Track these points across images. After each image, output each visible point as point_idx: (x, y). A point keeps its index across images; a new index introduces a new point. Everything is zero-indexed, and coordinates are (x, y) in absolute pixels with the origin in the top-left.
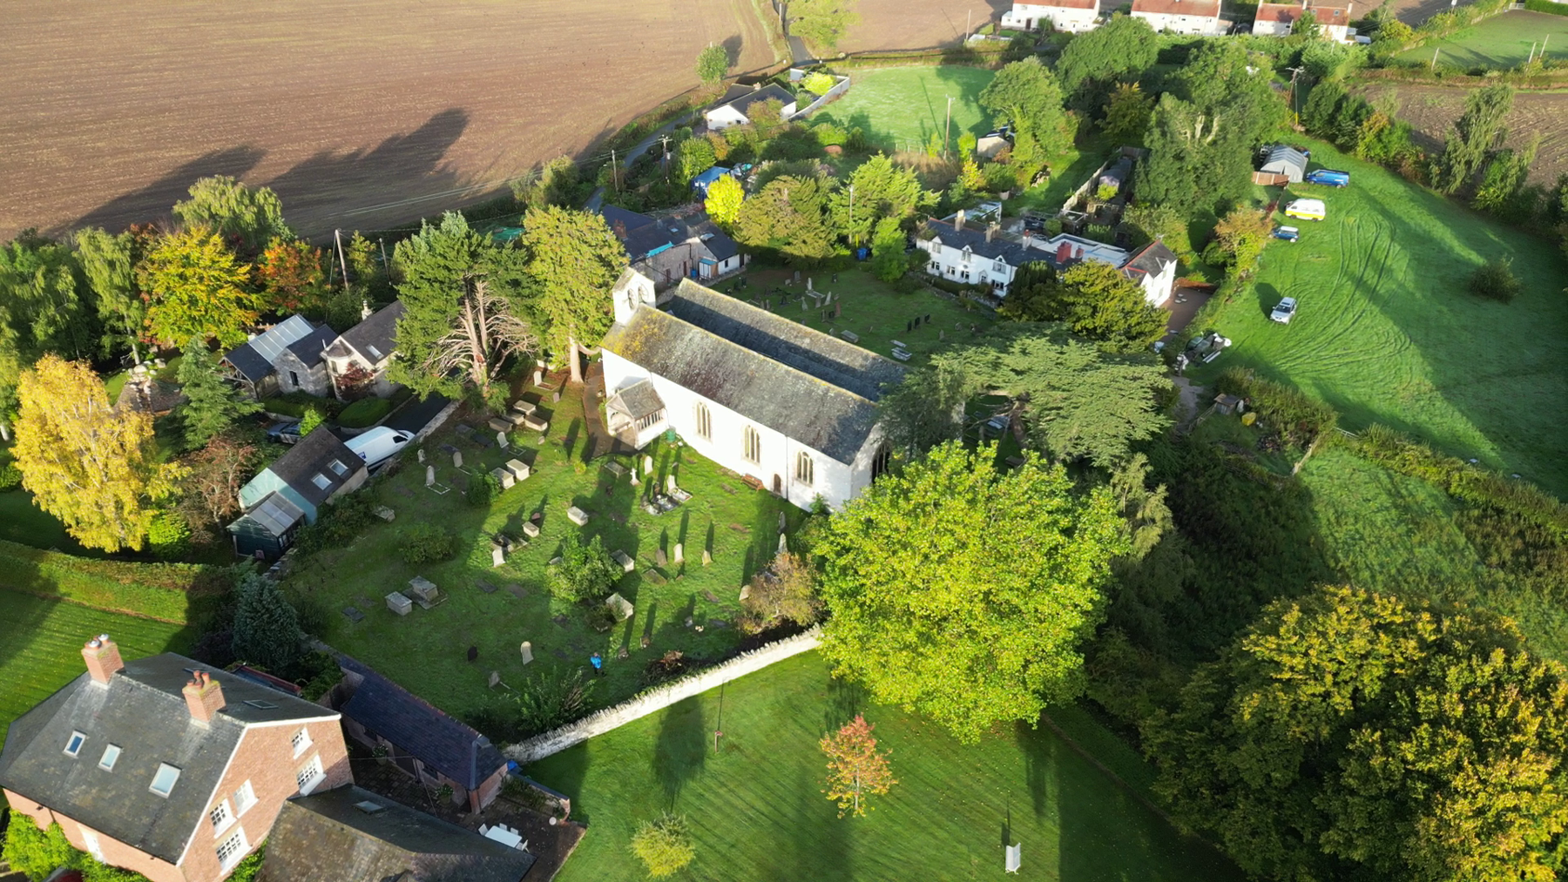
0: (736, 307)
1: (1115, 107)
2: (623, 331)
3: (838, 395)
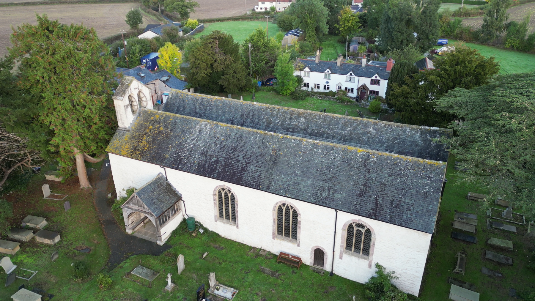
0: (226, 104)
1: (344, 16)
2: (128, 134)
3: (381, 159)
